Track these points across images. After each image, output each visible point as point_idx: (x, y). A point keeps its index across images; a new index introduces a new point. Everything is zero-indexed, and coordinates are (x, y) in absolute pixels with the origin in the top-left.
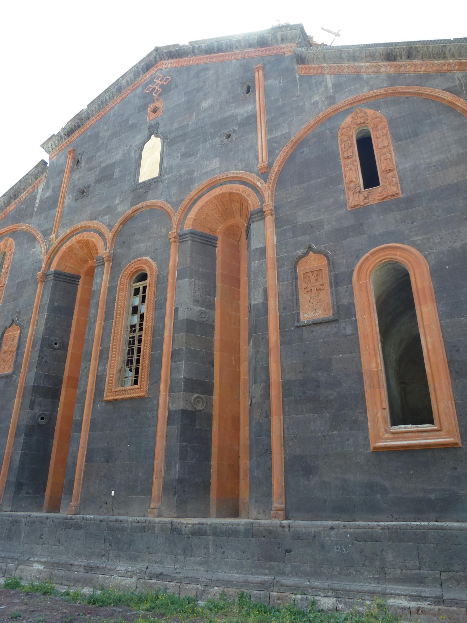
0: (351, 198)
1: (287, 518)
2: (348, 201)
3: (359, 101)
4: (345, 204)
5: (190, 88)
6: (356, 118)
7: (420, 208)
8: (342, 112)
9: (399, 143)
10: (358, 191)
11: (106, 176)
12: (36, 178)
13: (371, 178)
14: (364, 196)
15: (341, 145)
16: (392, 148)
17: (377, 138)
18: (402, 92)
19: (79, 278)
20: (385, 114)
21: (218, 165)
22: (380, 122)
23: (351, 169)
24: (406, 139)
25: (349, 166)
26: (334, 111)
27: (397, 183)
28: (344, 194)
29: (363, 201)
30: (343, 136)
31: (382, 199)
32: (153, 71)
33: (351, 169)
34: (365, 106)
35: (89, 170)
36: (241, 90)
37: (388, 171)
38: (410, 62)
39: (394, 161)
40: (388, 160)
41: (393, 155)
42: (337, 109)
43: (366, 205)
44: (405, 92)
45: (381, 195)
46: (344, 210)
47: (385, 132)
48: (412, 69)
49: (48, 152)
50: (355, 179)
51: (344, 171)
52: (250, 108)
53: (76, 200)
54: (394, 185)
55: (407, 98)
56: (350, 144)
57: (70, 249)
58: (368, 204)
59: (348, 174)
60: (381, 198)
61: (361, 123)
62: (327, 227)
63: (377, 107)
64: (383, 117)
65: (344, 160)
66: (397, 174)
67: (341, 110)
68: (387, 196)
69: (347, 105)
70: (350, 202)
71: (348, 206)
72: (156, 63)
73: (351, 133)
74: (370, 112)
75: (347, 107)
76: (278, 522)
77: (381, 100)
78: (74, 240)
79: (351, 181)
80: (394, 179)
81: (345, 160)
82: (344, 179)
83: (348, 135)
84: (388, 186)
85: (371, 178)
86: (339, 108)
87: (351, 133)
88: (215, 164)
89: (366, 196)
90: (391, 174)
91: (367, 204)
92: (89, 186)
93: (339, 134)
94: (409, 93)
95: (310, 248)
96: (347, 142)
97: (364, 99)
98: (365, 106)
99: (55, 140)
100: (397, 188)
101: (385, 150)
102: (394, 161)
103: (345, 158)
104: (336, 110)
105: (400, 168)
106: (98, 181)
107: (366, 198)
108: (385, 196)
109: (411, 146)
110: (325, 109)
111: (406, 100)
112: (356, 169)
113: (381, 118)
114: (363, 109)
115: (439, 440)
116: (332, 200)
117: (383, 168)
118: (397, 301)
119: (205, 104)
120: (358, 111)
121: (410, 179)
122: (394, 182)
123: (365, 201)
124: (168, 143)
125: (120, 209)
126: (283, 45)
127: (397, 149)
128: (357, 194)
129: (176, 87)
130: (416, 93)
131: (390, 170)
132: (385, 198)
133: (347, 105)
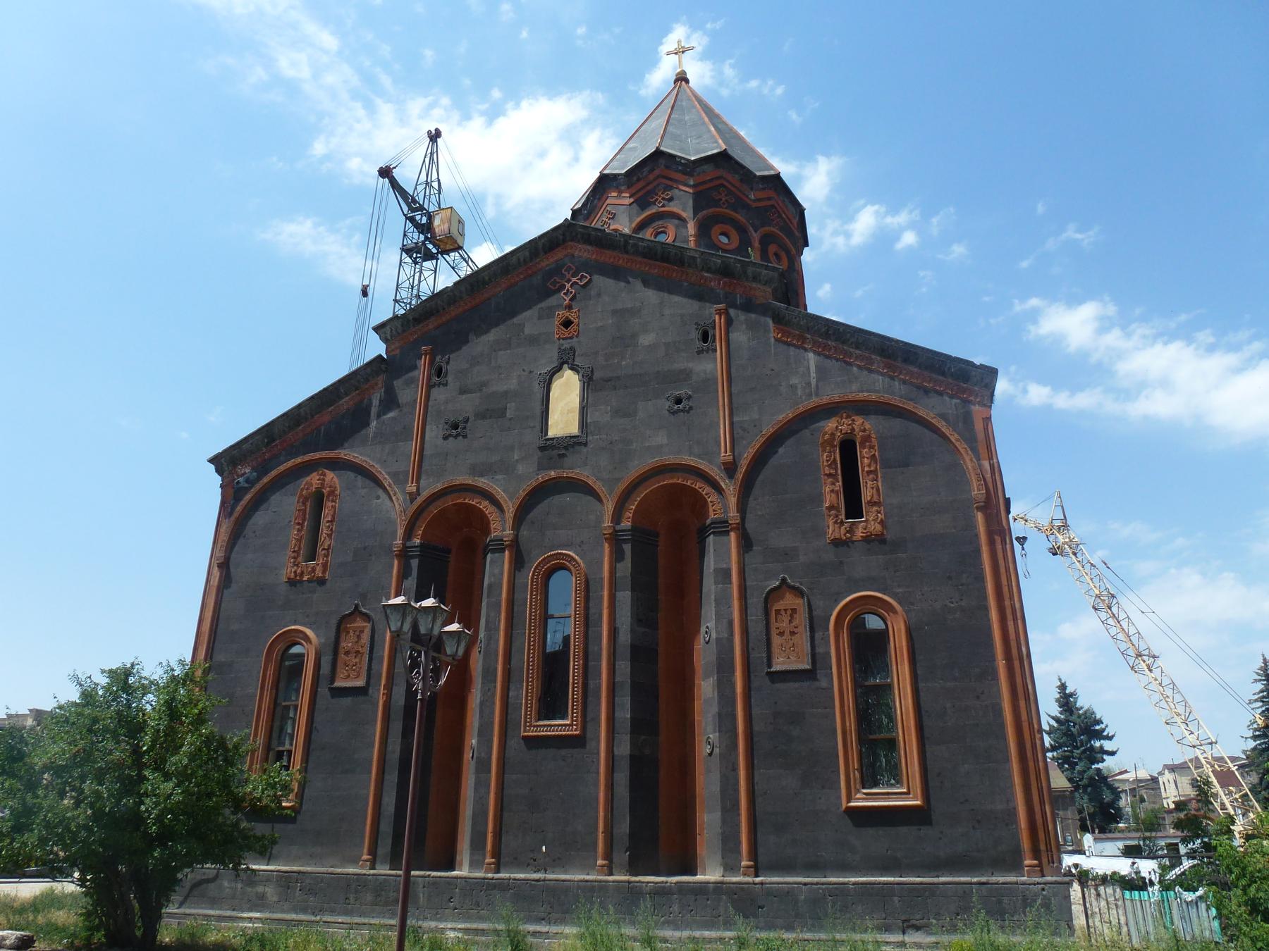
1: (757, 876)
5: (619, 306)
7: (904, 555)
11: (493, 412)
12: (367, 380)
13: (854, 509)
19: (449, 551)
21: (665, 441)
32: (559, 254)
35: (463, 391)
36: (695, 335)
49: (385, 340)
52: (708, 366)
53: (445, 438)
57: (443, 512)
62: (802, 558)
72: (564, 241)
76: (750, 879)
78: (449, 501)
85: (854, 509)
88: (661, 439)
92: (467, 421)
95: (784, 580)
99: (398, 324)
106: (481, 416)
115: (963, 879)
118: (869, 650)
119: (646, 340)
124: (589, 383)
125: (521, 469)
126: (754, 285)
129: (599, 295)
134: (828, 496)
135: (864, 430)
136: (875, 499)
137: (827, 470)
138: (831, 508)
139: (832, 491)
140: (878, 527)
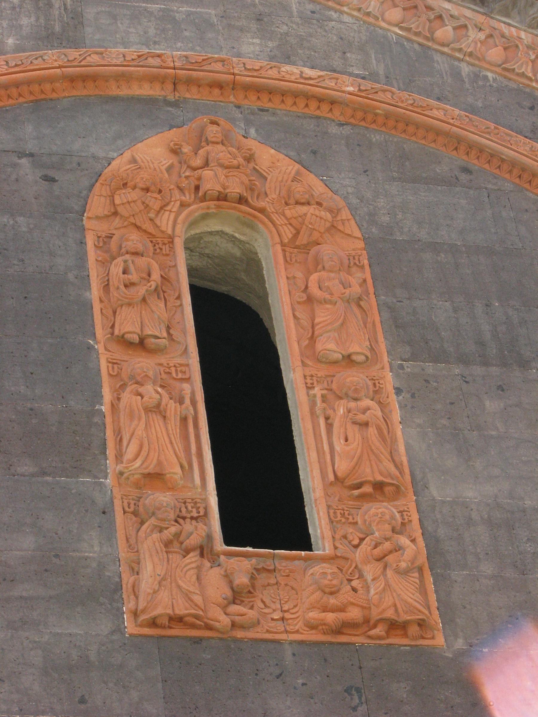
0: (150, 570)
2: (127, 579)
3: (220, 86)
4: (104, 593)
6: (198, 162)
8: (115, 99)
9: (430, 368)
10: (194, 540)
13: (262, 502)
14: (228, 577)
15: (105, 264)
16: (389, 381)
17: (310, 300)
18: (447, 134)
20: (354, 201)
22: (328, 230)
23: (157, 409)
24: (464, 360)
25: (149, 389)
26: (72, 79)
27: (420, 570)
28: (108, 531)
29: (224, 608)
30: (117, 222)
31: (338, 631)
33: (157, 409)
34: (248, 123)
37: (367, 489)
38: (480, 19)
39: (402, 449)
40: (372, 431)
41: (397, 415)
42: (94, 78)
43: (239, 634)
44: (459, 140)
45: (333, 601)
46: (104, 627)
47: (356, 289)
48: (495, 54)
50: (178, 470)
51: (114, 407)
54: (406, 572)
55: (466, 170)
56: (156, 276)
58: (251, 634)
59: (140, 432)
61: (222, 197)
63: (313, 157)
64: (345, 214)
65: (113, 346)
66: (415, 517)
67: (114, 90)
68: (367, 621)
69: (152, 79)
71: (128, 606)
73: (165, 221)
74: (276, 163)
75: (146, 90)
77: (334, 130)
79: (155, 478)
80: (404, 541)
81: (119, 353)
82: (111, 452)
83: (148, 226)
84: (370, 571)
85: (262, 502)
86: (106, 78)
87: (165, 221)
89: (242, 580)
90: (379, 510)
91: (242, 627)
93: (97, 205)
94: (481, 150)
96: (141, 261)
97: (248, 88)
98: (248, 123)
100: (423, 590)
101: (353, 377)
102: (402, 449)
103: (124, 342)
104: (84, 78)
105: (434, 491)
107: (237, 596)
108: (354, 614)
110: (19, 49)
111: (464, 177)
112: (184, 420)
113: (334, 212)
114: (238, 132)
116: (27, 543)
120: (212, 131)
121: (487, 568)
123: (234, 608)
127: (414, 393)
128: (193, 557)
130: (513, 164)
131: (379, 486)
132: (352, 625)
133: (152, 79)
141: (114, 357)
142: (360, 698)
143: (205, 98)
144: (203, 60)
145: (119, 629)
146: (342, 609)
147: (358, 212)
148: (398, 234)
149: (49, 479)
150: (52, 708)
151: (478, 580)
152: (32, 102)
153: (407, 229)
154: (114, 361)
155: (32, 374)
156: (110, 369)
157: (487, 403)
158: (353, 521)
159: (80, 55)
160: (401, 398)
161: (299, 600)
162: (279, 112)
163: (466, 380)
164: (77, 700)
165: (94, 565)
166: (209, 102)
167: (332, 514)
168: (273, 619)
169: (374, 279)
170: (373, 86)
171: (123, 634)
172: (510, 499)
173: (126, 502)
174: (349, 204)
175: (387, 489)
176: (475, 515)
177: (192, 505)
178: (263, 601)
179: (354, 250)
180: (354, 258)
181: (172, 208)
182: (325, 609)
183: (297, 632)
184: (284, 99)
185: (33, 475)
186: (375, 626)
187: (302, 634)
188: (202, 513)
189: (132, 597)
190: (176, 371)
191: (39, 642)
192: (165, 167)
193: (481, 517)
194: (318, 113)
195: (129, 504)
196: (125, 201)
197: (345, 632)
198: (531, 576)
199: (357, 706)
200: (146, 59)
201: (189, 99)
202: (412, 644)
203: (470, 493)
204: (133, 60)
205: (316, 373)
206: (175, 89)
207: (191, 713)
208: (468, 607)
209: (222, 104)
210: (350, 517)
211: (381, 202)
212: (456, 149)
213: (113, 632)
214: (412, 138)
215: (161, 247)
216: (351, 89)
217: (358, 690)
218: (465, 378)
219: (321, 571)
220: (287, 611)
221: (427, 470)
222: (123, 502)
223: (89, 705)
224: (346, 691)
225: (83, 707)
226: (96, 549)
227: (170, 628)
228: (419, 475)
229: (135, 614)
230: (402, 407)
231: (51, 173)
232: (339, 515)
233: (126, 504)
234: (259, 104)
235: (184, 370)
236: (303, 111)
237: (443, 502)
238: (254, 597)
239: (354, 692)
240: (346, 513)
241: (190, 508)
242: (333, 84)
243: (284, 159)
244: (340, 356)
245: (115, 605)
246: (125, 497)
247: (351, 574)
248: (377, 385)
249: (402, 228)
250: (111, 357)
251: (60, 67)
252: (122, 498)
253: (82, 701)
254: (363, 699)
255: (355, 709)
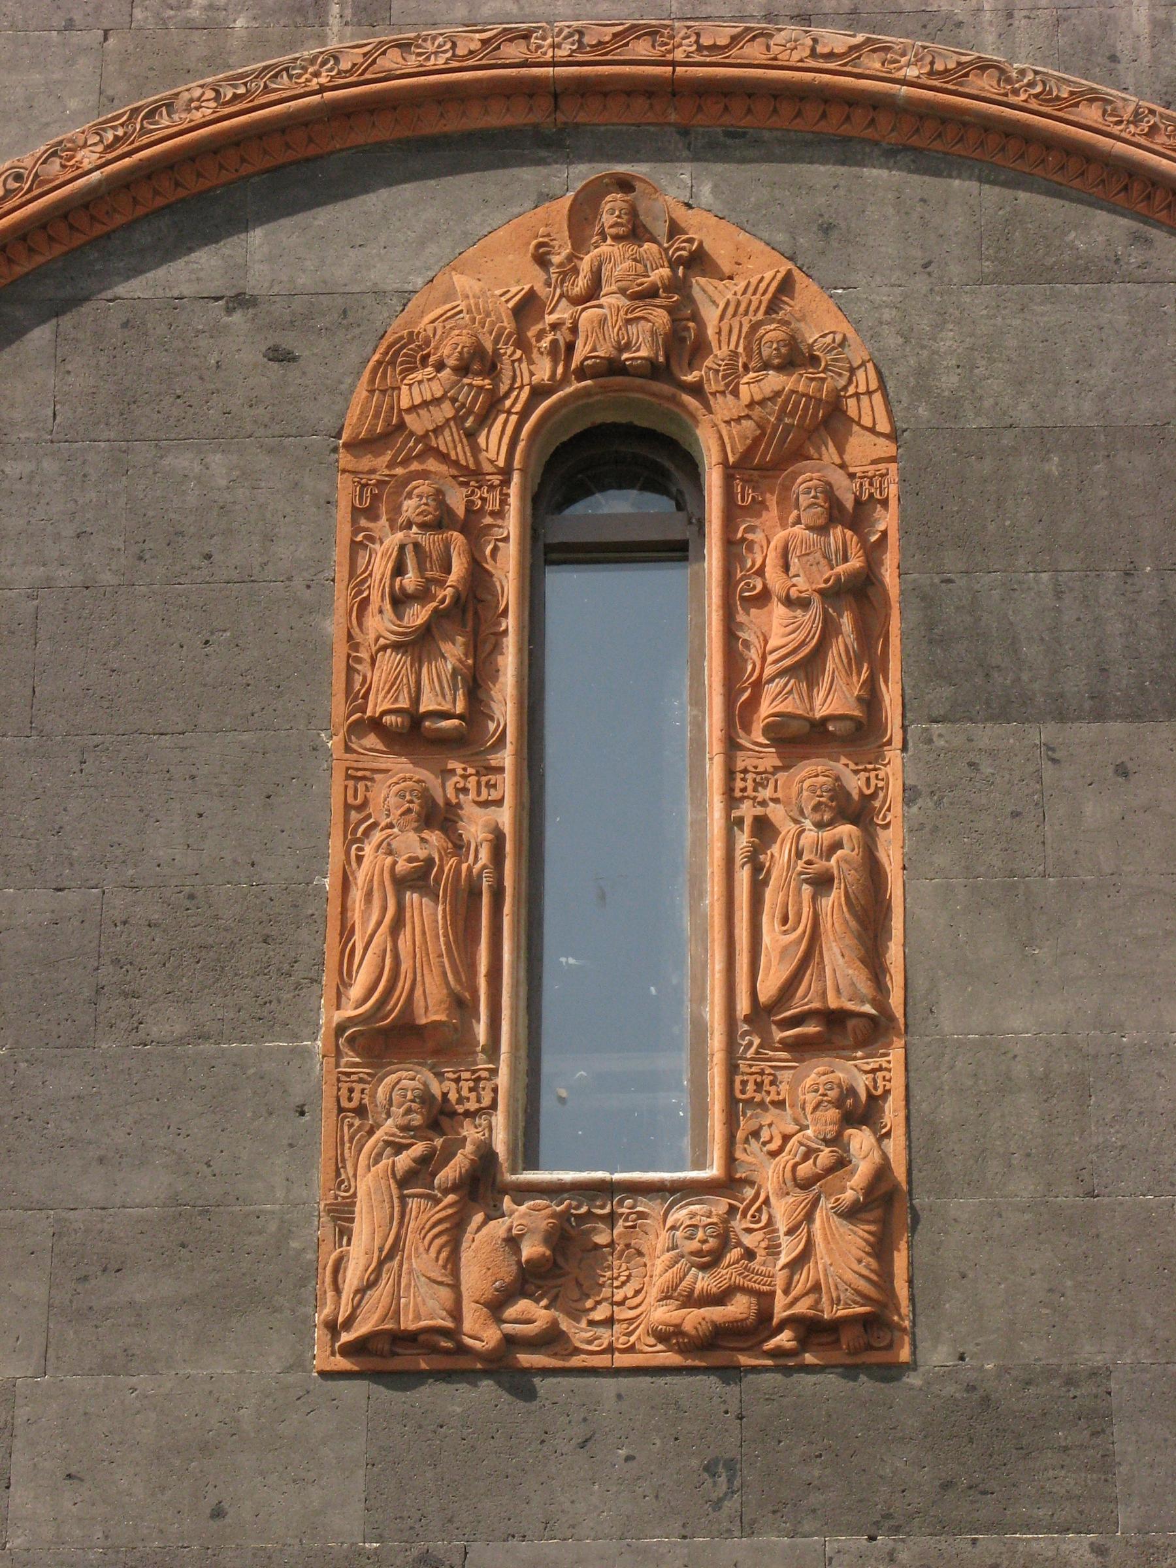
45: (704, 1282)
60: (694, 1319)
70: (352, 1277)
82: (329, 978)
109: (1094, 810)
110: (257, 41)
117: (768, 988)
121: (1024, 1187)
122: (862, 1170)
134: (368, 919)
135: (795, 357)
136: (840, 979)
137: (386, 687)
138: (388, 1037)
139: (418, 878)
140: (840, 1258)
141: (360, 765)
142: (730, 1481)
143: (615, 120)
144: (615, 35)
145: (300, 1363)
146: (720, 1299)
147: (895, 370)
148: (970, 415)
149: (207, 1047)
150: (161, 1531)
151: (1001, 1216)
152: (267, 171)
153: (991, 401)
154: (360, 774)
155: (201, 815)
156: (350, 792)
157: (1088, 809)
158: (776, 1098)
159: (365, 55)
160: (915, 809)
161: (646, 1279)
162: (766, 135)
163: (1055, 756)
164: (208, 1511)
165: (273, 1227)
166: (625, 128)
167: (738, 1086)
168: (591, 1323)
169: (904, 531)
170: (964, 59)
171: (306, 1370)
172: (1095, 1029)
173: (345, 1087)
174: (879, 350)
175: (851, 1023)
176: (1019, 1070)
177: (471, 1084)
178: (579, 1285)
179: (874, 462)
180: (871, 484)
181: (513, 405)
182: (691, 1300)
183: (631, 1349)
184: (778, 106)
185: (181, 1041)
186: (779, 1329)
187: (642, 1352)
188: (486, 1102)
189: (330, 1294)
190: (479, 783)
191: (155, 1395)
192: (511, 304)
193: (1031, 1073)
194: (846, 130)
195: (351, 1090)
196: (417, 401)
197: (725, 1344)
198: (1106, 1200)
199: (720, 1500)
200: (498, 47)
201: (584, 125)
202: (847, 1362)
203: (1020, 1022)
204: (471, 52)
205: (756, 762)
206: (556, 107)
207: (411, 1528)
208: (971, 1275)
209: (652, 129)
210: (773, 1089)
211: (948, 340)
212: (1126, 188)
213: (287, 1370)
214: (1035, 171)
215: (485, 495)
216: (912, 72)
217: (730, 1465)
218: (1053, 750)
219: (688, 1223)
220: (621, 1303)
221: (941, 973)
222: (339, 1089)
223: (228, 1520)
224: (706, 1469)
225: (214, 1525)
226: (280, 1194)
227: (394, 1354)
228: (921, 983)
229: (333, 1328)
230: (913, 829)
231: (288, 341)
232: (751, 1087)
233: (344, 1092)
234: (726, 119)
235: (492, 782)
236: (815, 129)
237: (960, 1044)
238: (563, 1275)
239: (721, 1469)
240: (767, 1082)
241: (465, 1093)
242: (878, 65)
243: (762, 252)
244: (806, 727)
245: (302, 1310)
246: (344, 1078)
247: (753, 1216)
248: (873, 782)
249: (981, 398)
250: (355, 765)
251: (322, 89)
252: (339, 1080)
253: (218, 1513)
254: (737, 1483)
255: (717, 1505)
